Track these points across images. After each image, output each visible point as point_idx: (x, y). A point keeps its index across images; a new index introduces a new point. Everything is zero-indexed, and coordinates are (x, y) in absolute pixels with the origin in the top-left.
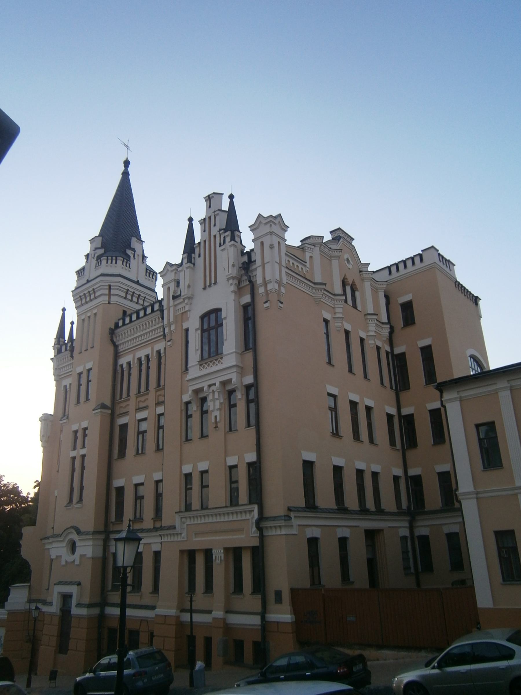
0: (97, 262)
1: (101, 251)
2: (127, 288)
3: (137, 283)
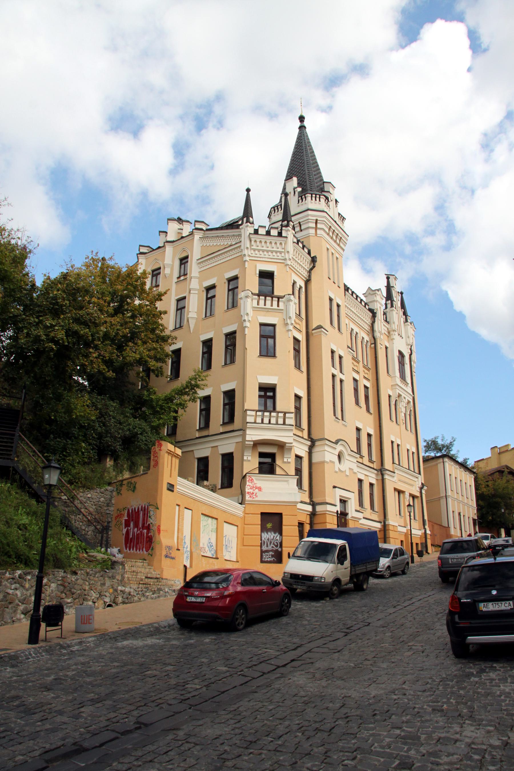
0: (300, 198)
2: (330, 225)
3: (335, 222)
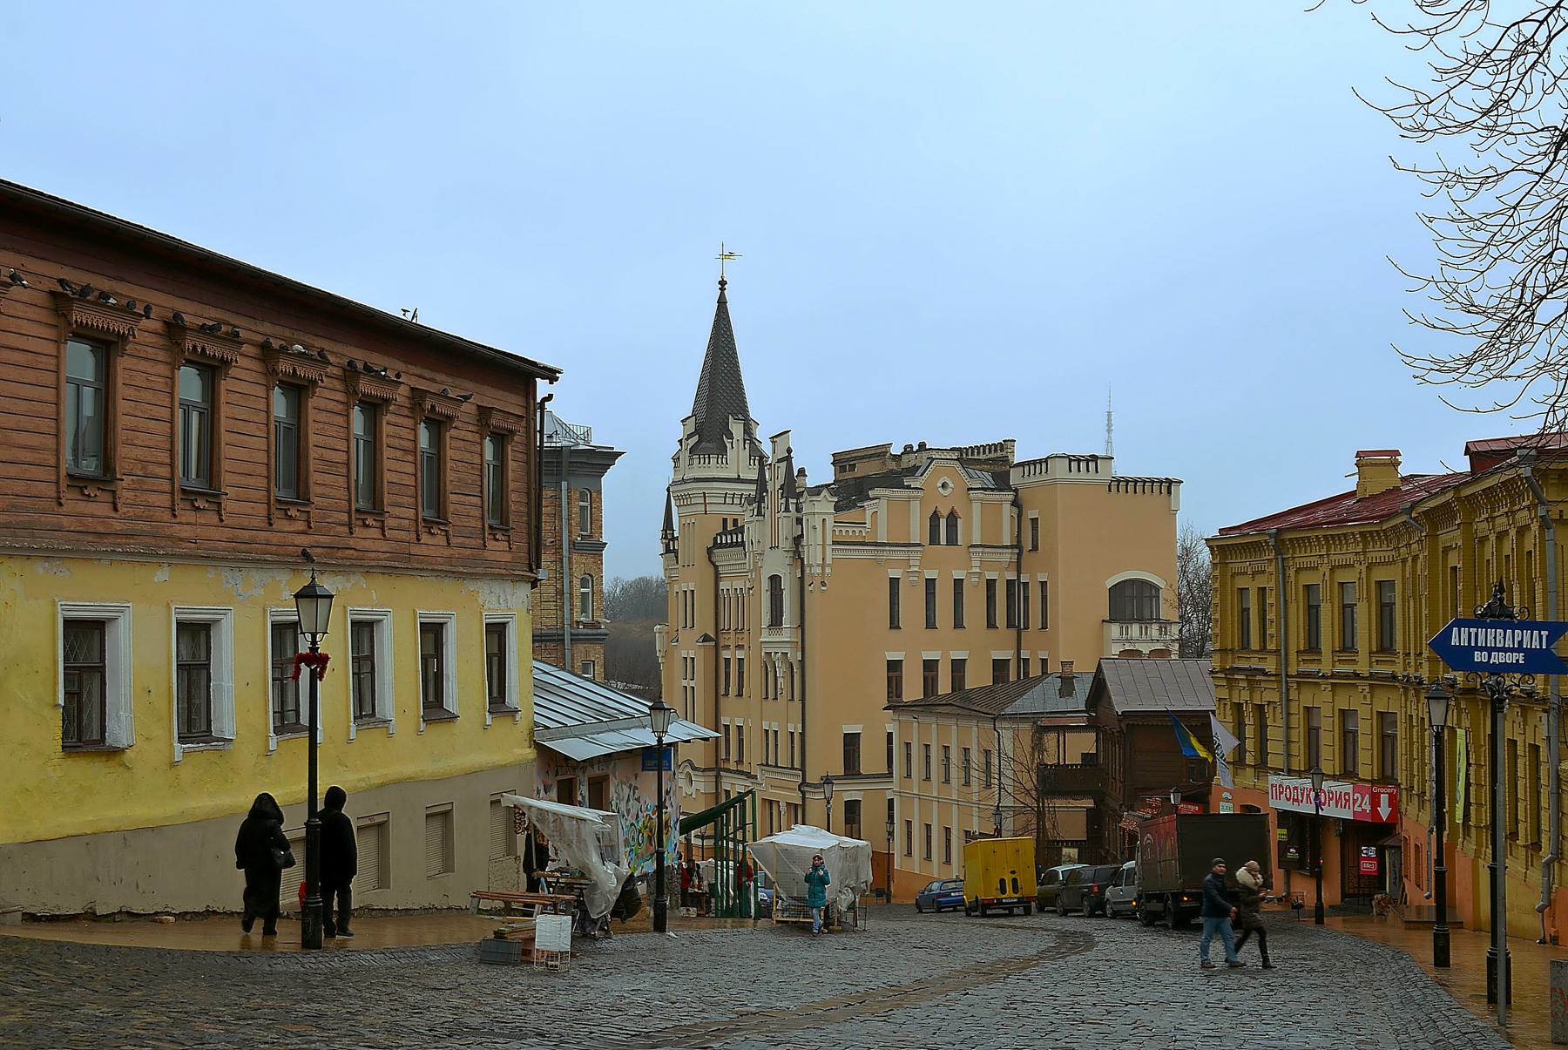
1: (696, 439)
3: (738, 480)
